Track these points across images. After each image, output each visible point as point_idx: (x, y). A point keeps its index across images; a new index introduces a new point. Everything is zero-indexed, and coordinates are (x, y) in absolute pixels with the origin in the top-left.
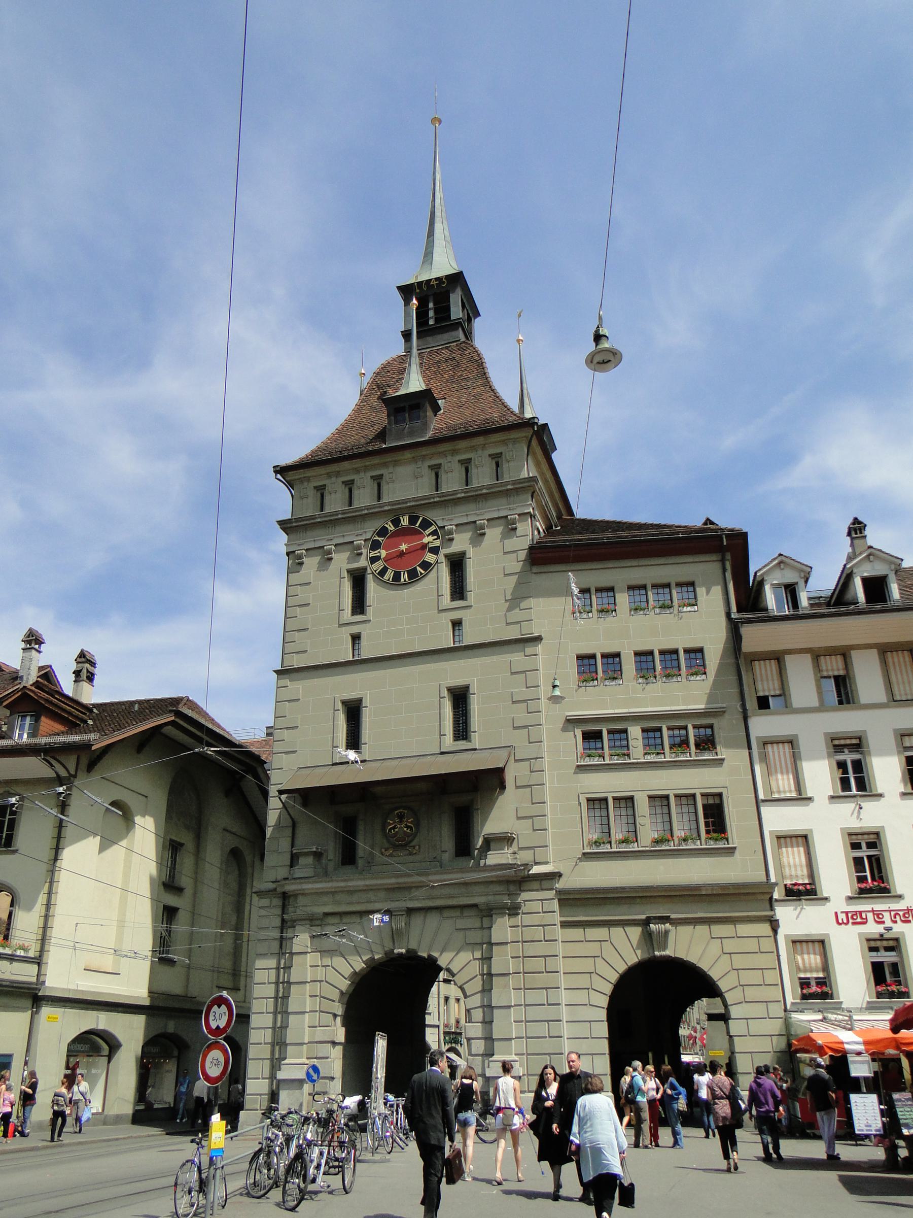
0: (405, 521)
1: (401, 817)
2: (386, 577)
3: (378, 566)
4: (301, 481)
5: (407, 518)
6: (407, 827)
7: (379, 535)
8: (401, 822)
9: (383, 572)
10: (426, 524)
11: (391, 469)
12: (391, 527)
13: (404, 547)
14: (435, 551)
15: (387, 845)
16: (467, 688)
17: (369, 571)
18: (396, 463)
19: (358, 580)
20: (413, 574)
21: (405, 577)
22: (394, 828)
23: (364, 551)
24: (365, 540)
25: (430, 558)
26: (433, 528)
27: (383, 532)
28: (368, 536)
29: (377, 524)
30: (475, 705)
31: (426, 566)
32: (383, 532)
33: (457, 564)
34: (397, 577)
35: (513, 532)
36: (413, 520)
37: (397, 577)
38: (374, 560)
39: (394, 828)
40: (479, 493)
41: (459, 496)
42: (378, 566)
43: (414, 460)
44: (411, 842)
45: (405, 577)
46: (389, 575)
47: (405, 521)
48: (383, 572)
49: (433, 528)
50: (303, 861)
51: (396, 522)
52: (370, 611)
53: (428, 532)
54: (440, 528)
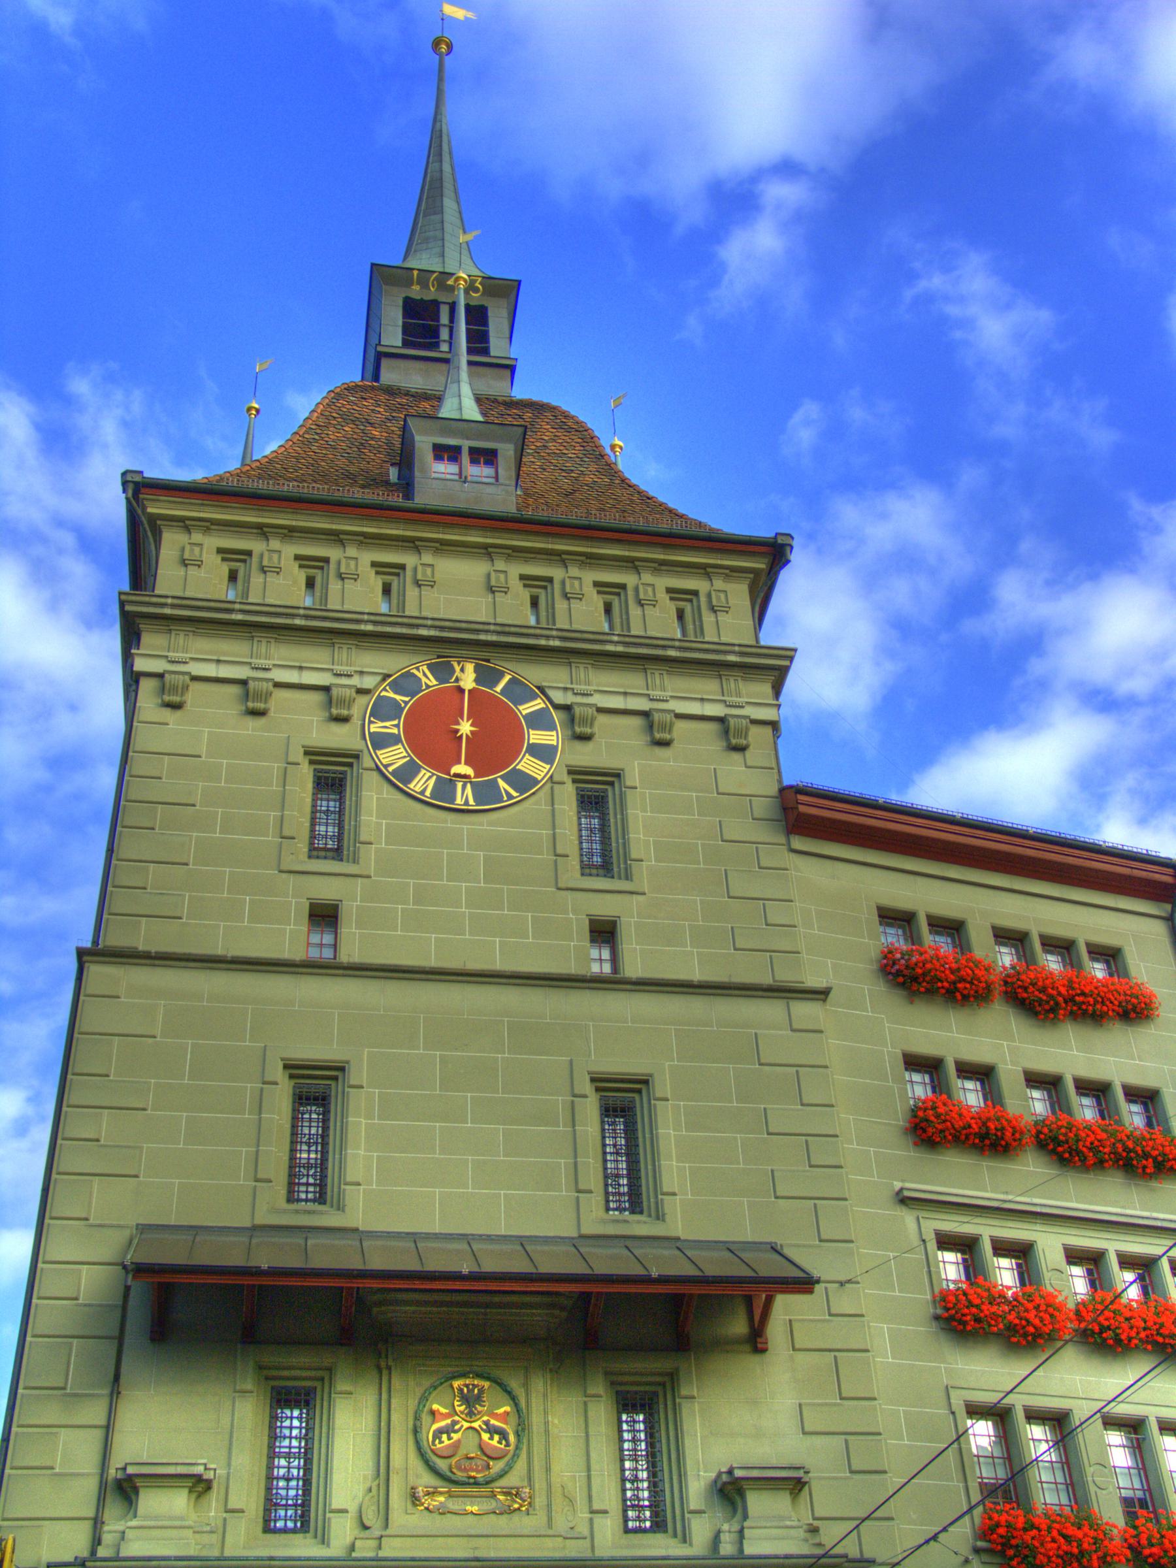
1: (471, 1400)
2: (416, 786)
3: (395, 756)
4: (185, 525)
6: (492, 1431)
7: (396, 687)
8: (471, 1414)
9: (407, 772)
11: (427, 558)
12: (429, 681)
14: (543, 753)
15: (426, 1480)
16: (643, 1083)
17: (367, 762)
18: (443, 548)
19: (333, 776)
20: (486, 793)
21: (464, 796)
22: (448, 1430)
23: (356, 711)
24: (361, 691)
26: (538, 704)
27: (405, 684)
28: (368, 682)
29: (394, 662)
30: (671, 1130)
31: (523, 782)
33: (597, 794)
34: (445, 789)
35: (736, 757)
36: (487, 676)
37: (445, 789)
38: (381, 741)
39: (448, 1430)
40: (660, 652)
41: (610, 648)
43: (487, 552)
44: (502, 1474)
45: (464, 796)
46: (424, 782)
48: (407, 772)
49: (538, 704)
50: (152, 1502)
51: (442, 671)
52: (369, 858)
53: (526, 709)
54: (557, 707)
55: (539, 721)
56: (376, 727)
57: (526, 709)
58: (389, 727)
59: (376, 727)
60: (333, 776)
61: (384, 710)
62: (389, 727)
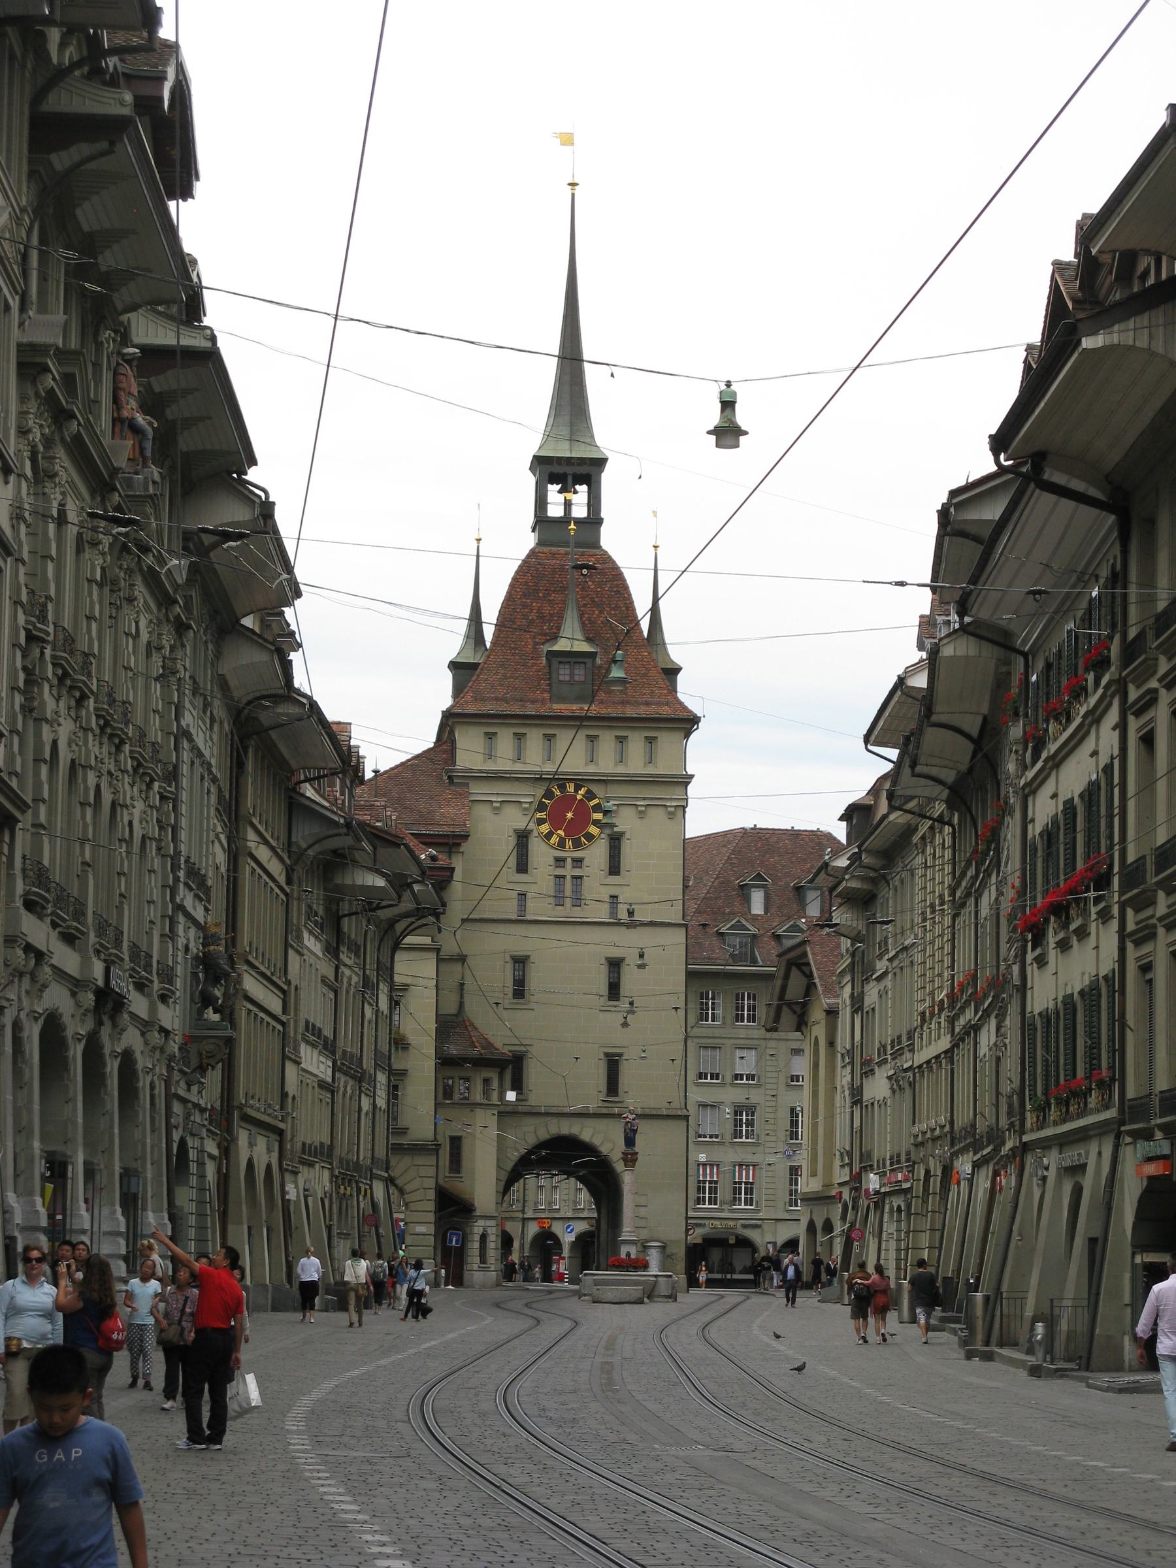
0: (571, 788)
2: (552, 841)
3: (545, 828)
5: (572, 785)
9: (549, 836)
10: (590, 795)
13: (570, 815)
17: (535, 833)
25: (593, 830)
26: (596, 801)
31: (590, 837)
32: (548, 794)
38: (540, 822)
42: (545, 828)
47: (571, 788)
48: (549, 836)
49: (596, 801)
51: (562, 787)
53: (592, 803)
55: (597, 808)
56: (539, 815)
57: (592, 803)
58: (542, 815)
59: (539, 815)
60: (523, 838)
61: (541, 807)
62: (542, 815)
